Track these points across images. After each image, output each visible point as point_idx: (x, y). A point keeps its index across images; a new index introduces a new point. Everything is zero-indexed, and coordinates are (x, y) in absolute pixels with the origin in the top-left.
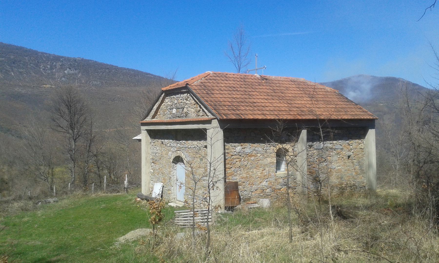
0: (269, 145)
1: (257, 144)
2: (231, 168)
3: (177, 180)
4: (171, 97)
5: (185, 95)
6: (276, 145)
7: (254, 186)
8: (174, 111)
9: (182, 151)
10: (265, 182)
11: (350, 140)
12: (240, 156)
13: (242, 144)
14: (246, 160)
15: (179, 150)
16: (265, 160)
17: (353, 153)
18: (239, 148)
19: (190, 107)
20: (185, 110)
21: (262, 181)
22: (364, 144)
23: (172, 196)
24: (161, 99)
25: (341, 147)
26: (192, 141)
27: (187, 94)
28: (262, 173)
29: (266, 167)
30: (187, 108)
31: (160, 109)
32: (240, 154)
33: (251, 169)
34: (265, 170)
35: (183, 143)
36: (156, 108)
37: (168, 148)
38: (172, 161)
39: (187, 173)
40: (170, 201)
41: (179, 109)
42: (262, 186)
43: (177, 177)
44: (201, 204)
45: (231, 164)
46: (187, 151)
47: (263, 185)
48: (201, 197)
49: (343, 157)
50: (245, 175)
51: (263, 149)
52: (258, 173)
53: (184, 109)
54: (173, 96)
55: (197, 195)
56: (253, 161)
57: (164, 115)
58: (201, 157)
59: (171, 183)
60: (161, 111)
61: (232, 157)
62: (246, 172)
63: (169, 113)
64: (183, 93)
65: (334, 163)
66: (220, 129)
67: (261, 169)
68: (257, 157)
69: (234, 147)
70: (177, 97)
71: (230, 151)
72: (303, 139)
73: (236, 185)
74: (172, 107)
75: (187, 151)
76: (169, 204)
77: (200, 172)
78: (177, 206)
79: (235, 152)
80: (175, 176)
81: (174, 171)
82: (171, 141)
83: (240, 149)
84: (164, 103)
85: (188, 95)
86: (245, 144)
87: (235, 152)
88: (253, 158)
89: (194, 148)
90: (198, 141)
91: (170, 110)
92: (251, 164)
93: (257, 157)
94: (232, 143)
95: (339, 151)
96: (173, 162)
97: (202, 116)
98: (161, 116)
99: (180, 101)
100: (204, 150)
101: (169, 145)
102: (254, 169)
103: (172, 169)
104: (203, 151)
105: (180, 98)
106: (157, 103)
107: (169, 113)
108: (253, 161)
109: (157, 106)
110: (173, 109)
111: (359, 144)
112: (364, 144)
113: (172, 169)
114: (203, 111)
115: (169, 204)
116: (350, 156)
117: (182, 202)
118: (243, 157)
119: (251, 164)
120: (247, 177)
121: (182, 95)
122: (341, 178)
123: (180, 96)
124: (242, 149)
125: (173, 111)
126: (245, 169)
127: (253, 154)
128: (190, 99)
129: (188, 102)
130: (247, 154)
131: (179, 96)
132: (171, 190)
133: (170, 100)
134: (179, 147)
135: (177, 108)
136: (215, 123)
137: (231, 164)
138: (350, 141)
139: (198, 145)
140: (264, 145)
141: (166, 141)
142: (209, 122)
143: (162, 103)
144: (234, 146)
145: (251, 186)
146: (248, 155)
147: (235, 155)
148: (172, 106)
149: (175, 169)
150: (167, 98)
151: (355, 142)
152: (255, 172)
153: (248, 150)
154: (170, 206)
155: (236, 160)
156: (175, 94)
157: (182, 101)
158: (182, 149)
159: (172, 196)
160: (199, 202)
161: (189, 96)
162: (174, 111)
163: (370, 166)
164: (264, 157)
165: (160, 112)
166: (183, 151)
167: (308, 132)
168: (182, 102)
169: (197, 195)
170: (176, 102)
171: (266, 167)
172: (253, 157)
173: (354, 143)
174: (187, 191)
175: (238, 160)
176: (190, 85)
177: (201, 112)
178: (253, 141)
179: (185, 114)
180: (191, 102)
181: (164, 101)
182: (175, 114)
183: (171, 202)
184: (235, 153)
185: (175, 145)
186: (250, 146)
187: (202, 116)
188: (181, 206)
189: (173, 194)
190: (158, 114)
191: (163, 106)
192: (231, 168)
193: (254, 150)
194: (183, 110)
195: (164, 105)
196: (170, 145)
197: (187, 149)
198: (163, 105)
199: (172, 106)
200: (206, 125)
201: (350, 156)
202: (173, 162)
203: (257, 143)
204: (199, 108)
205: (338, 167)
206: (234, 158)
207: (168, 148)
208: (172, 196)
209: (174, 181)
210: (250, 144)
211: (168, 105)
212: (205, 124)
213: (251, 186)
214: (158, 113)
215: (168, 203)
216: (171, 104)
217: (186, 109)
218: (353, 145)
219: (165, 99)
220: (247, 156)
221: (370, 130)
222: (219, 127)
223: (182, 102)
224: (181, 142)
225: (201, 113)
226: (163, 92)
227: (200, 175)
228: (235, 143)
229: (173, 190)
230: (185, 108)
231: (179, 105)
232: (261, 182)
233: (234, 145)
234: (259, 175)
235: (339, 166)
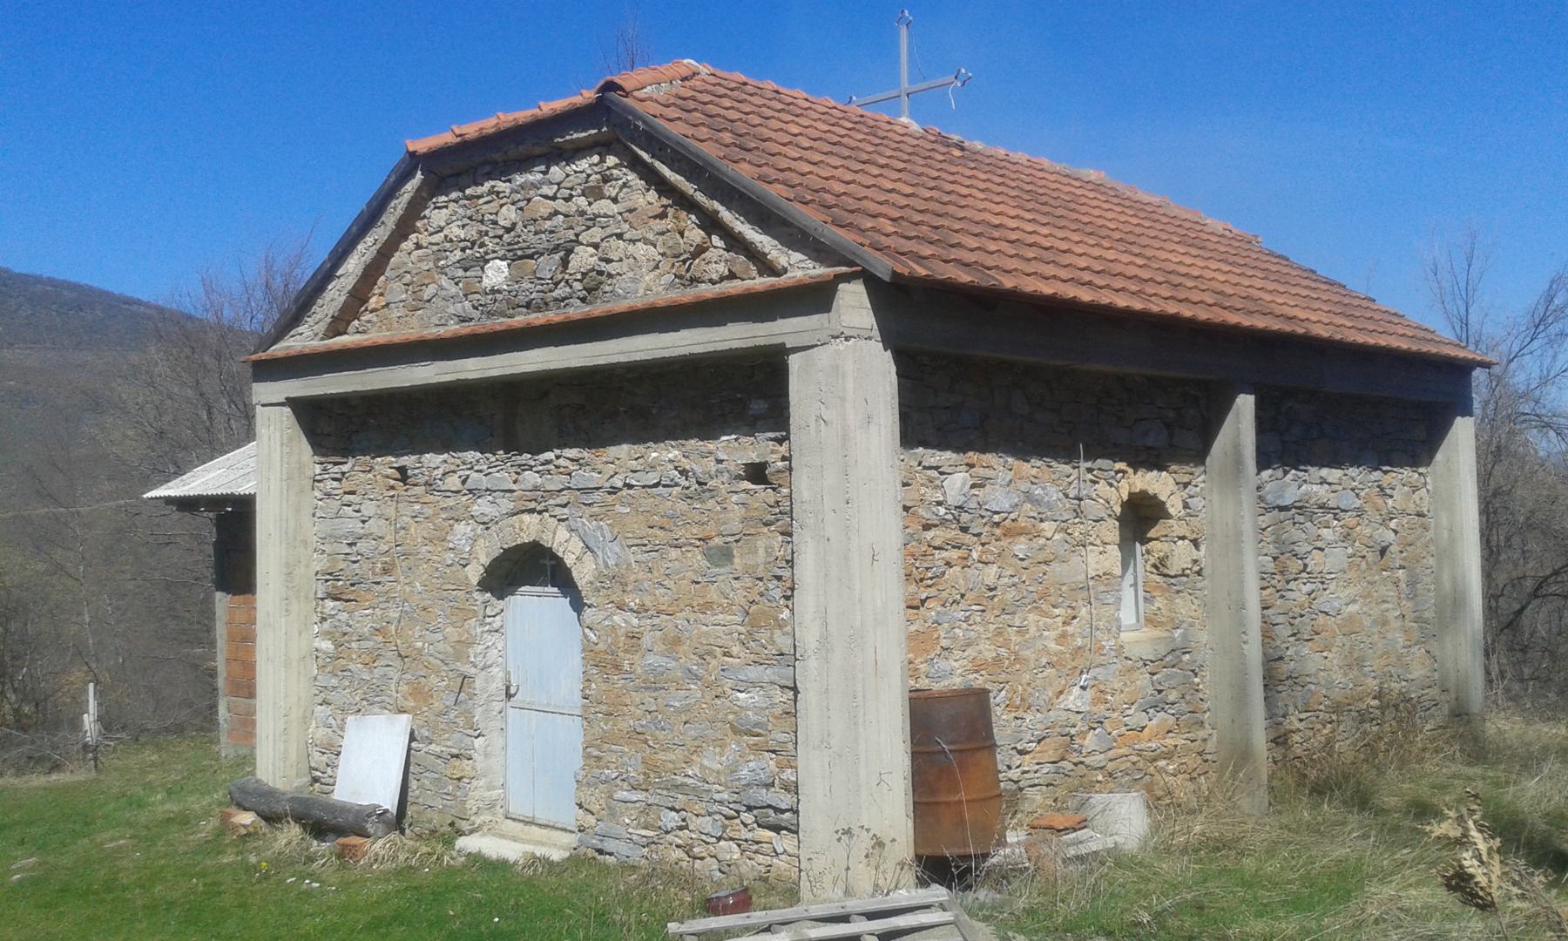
0: (1090, 470)
1: (1039, 463)
2: (923, 602)
3: (509, 696)
4: (468, 192)
5: (583, 164)
6: (1117, 472)
7: (1028, 717)
8: (496, 273)
9: (558, 511)
10: (1076, 691)
11: (1385, 468)
12: (964, 530)
13: (973, 456)
14: (991, 558)
15: (531, 511)
16: (1075, 559)
17: (1396, 532)
18: (958, 484)
19: (620, 236)
20: (584, 258)
21: (1063, 682)
22: (1428, 490)
23: (478, 794)
24: (399, 212)
25: (1358, 503)
26: (640, 448)
27: (596, 158)
28: (1064, 635)
29: (1080, 602)
30: (596, 246)
31: (388, 273)
32: (965, 517)
33: (1014, 613)
34: (1074, 618)
35: (561, 462)
36: (359, 271)
37: (451, 502)
38: (475, 580)
39: (602, 647)
40: (465, 826)
41: (531, 257)
42: (1064, 715)
43: (508, 673)
44: (719, 839)
45: (922, 580)
46: (595, 509)
47: (1071, 706)
48: (725, 796)
49: (1364, 553)
50: (988, 651)
51: (1066, 496)
52: (1046, 638)
53: (570, 251)
54: (488, 185)
55: (690, 781)
56: (1025, 564)
57: (420, 304)
58: (718, 541)
59: (468, 714)
60: (397, 286)
61: (929, 535)
62: (992, 627)
63: (453, 290)
64: (579, 151)
65: (1334, 582)
66: (877, 346)
67: (1057, 611)
68: (1042, 541)
69: (934, 473)
70: (522, 187)
71: (917, 496)
72: (1237, 448)
73: (972, 709)
74: (478, 252)
75: (595, 509)
76: (468, 844)
77: (707, 634)
78: (534, 860)
79: (939, 504)
80: (495, 670)
81: (490, 639)
82: (471, 456)
83: (964, 484)
84: (413, 237)
85: (602, 161)
86: (983, 457)
87: (939, 504)
88: (1021, 547)
89: (656, 485)
90: (693, 443)
91: (460, 273)
92: (1016, 580)
93: (1042, 541)
94: (926, 445)
95: (1349, 519)
96: (484, 586)
97: (722, 279)
98: (395, 313)
99: (546, 207)
100: (746, 491)
101: (453, 482)
102: (1029, 611)
103: (479, 630)
104: (735, 498)
105: (547, 190)
106: (369, 240)
107: (453, 290)
108: (1025, 564)
109: (368, 258)
110: (487, 261)
111: (1414, 492)
112: (1428, 490)
113: (479, 630)
114: (736, 243)
115: (468, 844)
116: (1387, 547)
117: (545, 832)
118: (979, 535)
119: (1016, 580)
120: (998, 660)
121: (554, 169)
122: (1359, 663)
123: (539, 176)
124: (973, 486)
125: (489, 272)
126: (988, 615)
127: (1023, 522)
128: (625, 185)
129: (604, 206)
130: (996, 518)
131: (534, 176)
132: (475, 756)
133: (461, 211)
134: (536, 489)
135: (517, 256)
136: (854, 304)
137: (922, 580)
138: (1386, 472)
139: (686, 464)
140: (1067, 468)
141: (432, 459)
142: (816, 298)
143: (405, 238)
144: (936, 468)
145: (1020, 713)
146: (997, 524)
147: (943, 522)
148: (482, 245)
149: (496, 626)
150: (444, 198)
151: (1400, 476)
152: (1033, 630)
153: (998, 498)
154: (478, 861)
155: (944, 554)
156: (503, 170)
157: (560, 205)
158: (562, 500)
159: (476, 794)
160: (709, 829)
161: (616, 166)
162: (496, 273)
163: (1457, 602)
164: (1068, 538)
165: (390, 288)
166: (566, 510)
167: (1260, 407)
168: (556, 213)
169: (690, 781)
170: (508, 215)
171: (1080, 602)
172: (1022, 539)
173: (1399, 477)
174: (598, 758)
175: (954, 554)
176: (627, 94)
177: (711, 254)
178: (1020, 444)
179: (578, 286)
180: (629, 204)
181: (419, 224)
182: (499, 291)
183: (472, 832)
184: (942, 511)
185: (504, 478)
186: (1010, 475)
187: (722, 279)
188: (556, 855)
189: (482, 783)
190: (373, 302)
191: (405, 256)
192: (923, 602)
193: (1028, 497)
194: (565, 263)
195: (418, 246)
196: (464, 482)
197: (596, 496)
198: (407, 245)
199: (482, 245)
200: (780, 322)
201: (1387, 547)
202: (484, 586)
203: (1041, 456)
204: (696, 235)
205: (1347, 604)
206: (937, 543)
207: (451, 502)
208: (476, 794)
209: (488, 702)
210: (1010, 460)
211: (448, 245)
212: (773, 319)
213: (1020, 713)
214: (373, 300)
215: (455, 838)
216: (472, 232)
217: (591, 250)
218: (1394, 493)
219: (427, 212)
220: (998, 531)
221: (1459, 419)
222: (876, 333)
223: (556, 213)
224: (549, 455)
225: (717, 259)
226: (414, 161)
227: (710, 653)
228: (942, 446)
229: (486, 755)
230: (578, 249)
231: (536, 233)
232: (1061, 692)
233: (933, 461)
234: (1053, 646)
235: (1354, 601)
